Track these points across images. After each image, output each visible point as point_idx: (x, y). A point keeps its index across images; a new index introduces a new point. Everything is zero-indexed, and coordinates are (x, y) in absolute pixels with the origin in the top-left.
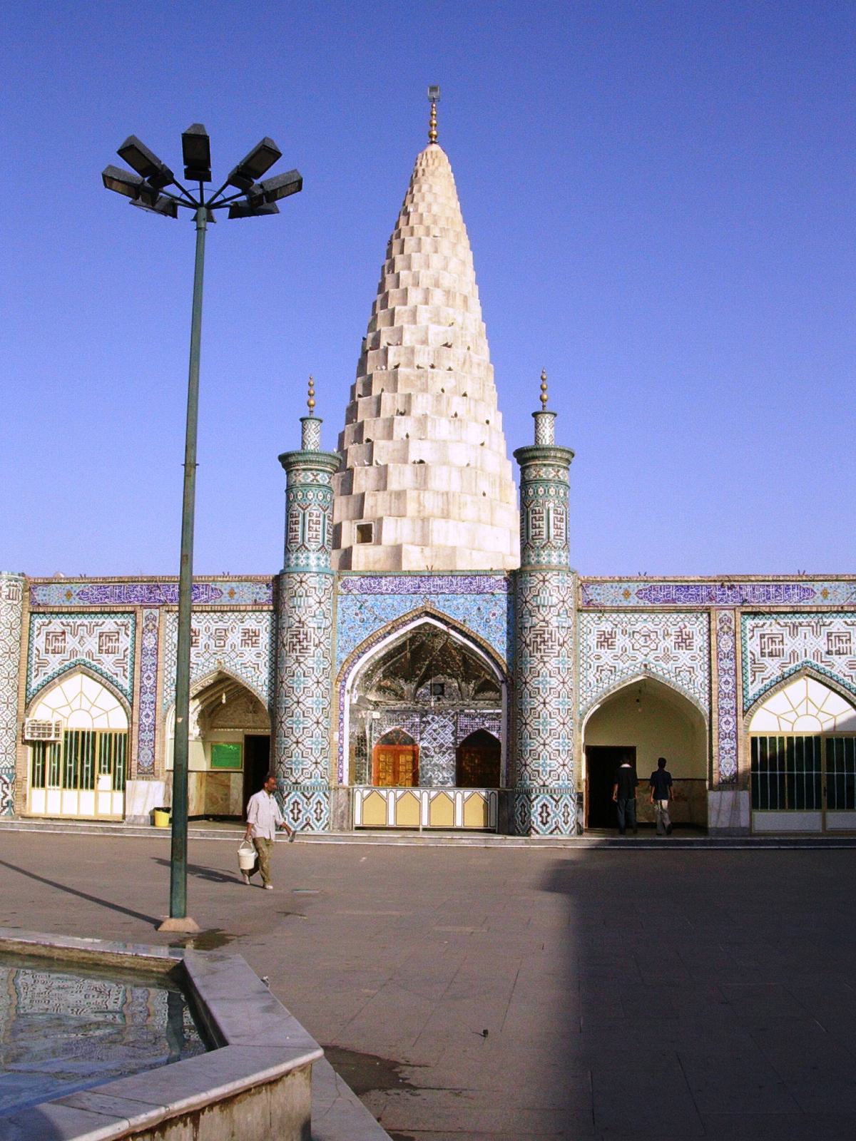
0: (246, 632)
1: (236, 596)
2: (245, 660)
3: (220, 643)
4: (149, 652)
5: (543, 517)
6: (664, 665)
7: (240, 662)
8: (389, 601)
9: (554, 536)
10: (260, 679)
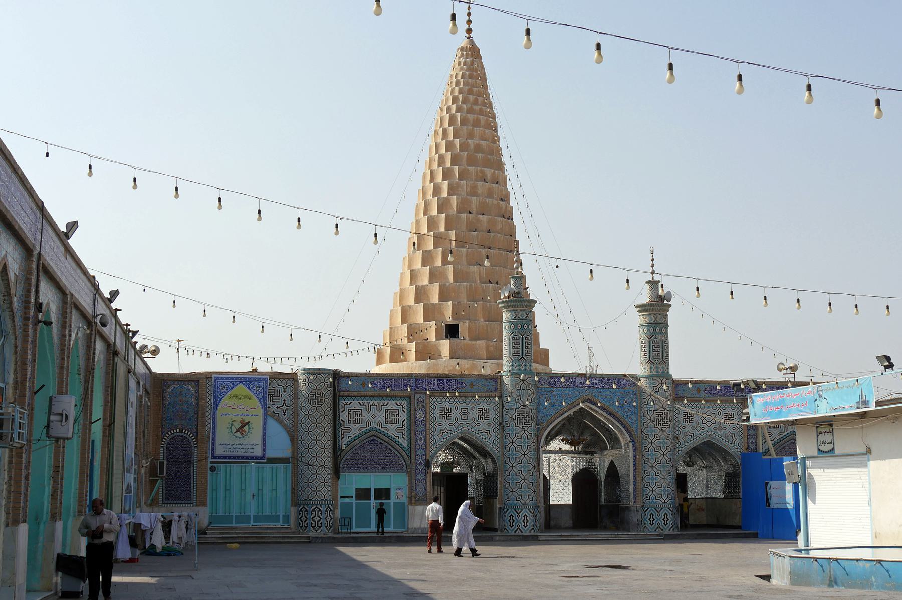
0: (480, 410)
1: (474, 387)
2: (481, 427)
3: (464, 417)
4: (421, 423)
6: (719, 433)
7: (478, 429)
8: (567, 392)
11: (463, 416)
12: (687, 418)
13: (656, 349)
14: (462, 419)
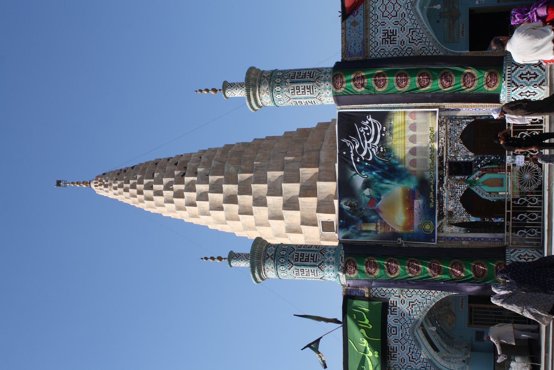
3: (394, 331)
5: (297, 87)
7: (408, 316)
9: (311, 94)
10: (421, 301)
11: (393, 333)
12: (390, 38)
13: (301, 91)
14: (396, 334)
